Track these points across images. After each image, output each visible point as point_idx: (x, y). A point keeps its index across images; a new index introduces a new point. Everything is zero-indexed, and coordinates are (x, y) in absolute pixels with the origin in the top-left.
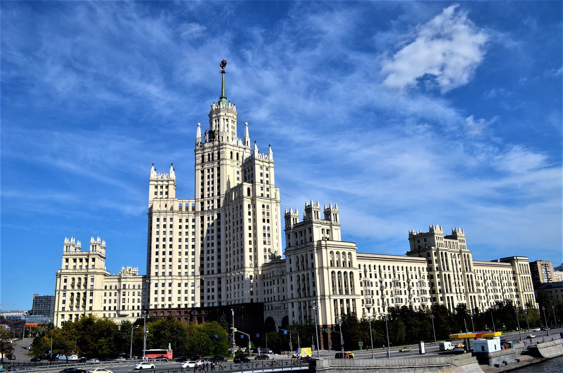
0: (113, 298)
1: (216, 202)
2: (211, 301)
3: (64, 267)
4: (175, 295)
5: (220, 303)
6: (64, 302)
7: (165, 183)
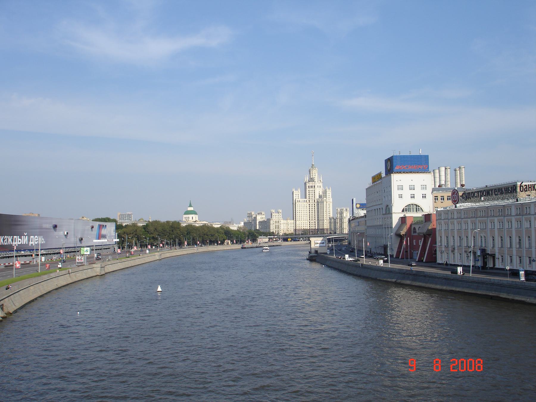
0: (285, 226)
1: (313, 200)
2: (312, 227)
3: (273, 218)
4: (303, 226)
5: (315, 228)
6: (274, 227)
7: (298, 194)
